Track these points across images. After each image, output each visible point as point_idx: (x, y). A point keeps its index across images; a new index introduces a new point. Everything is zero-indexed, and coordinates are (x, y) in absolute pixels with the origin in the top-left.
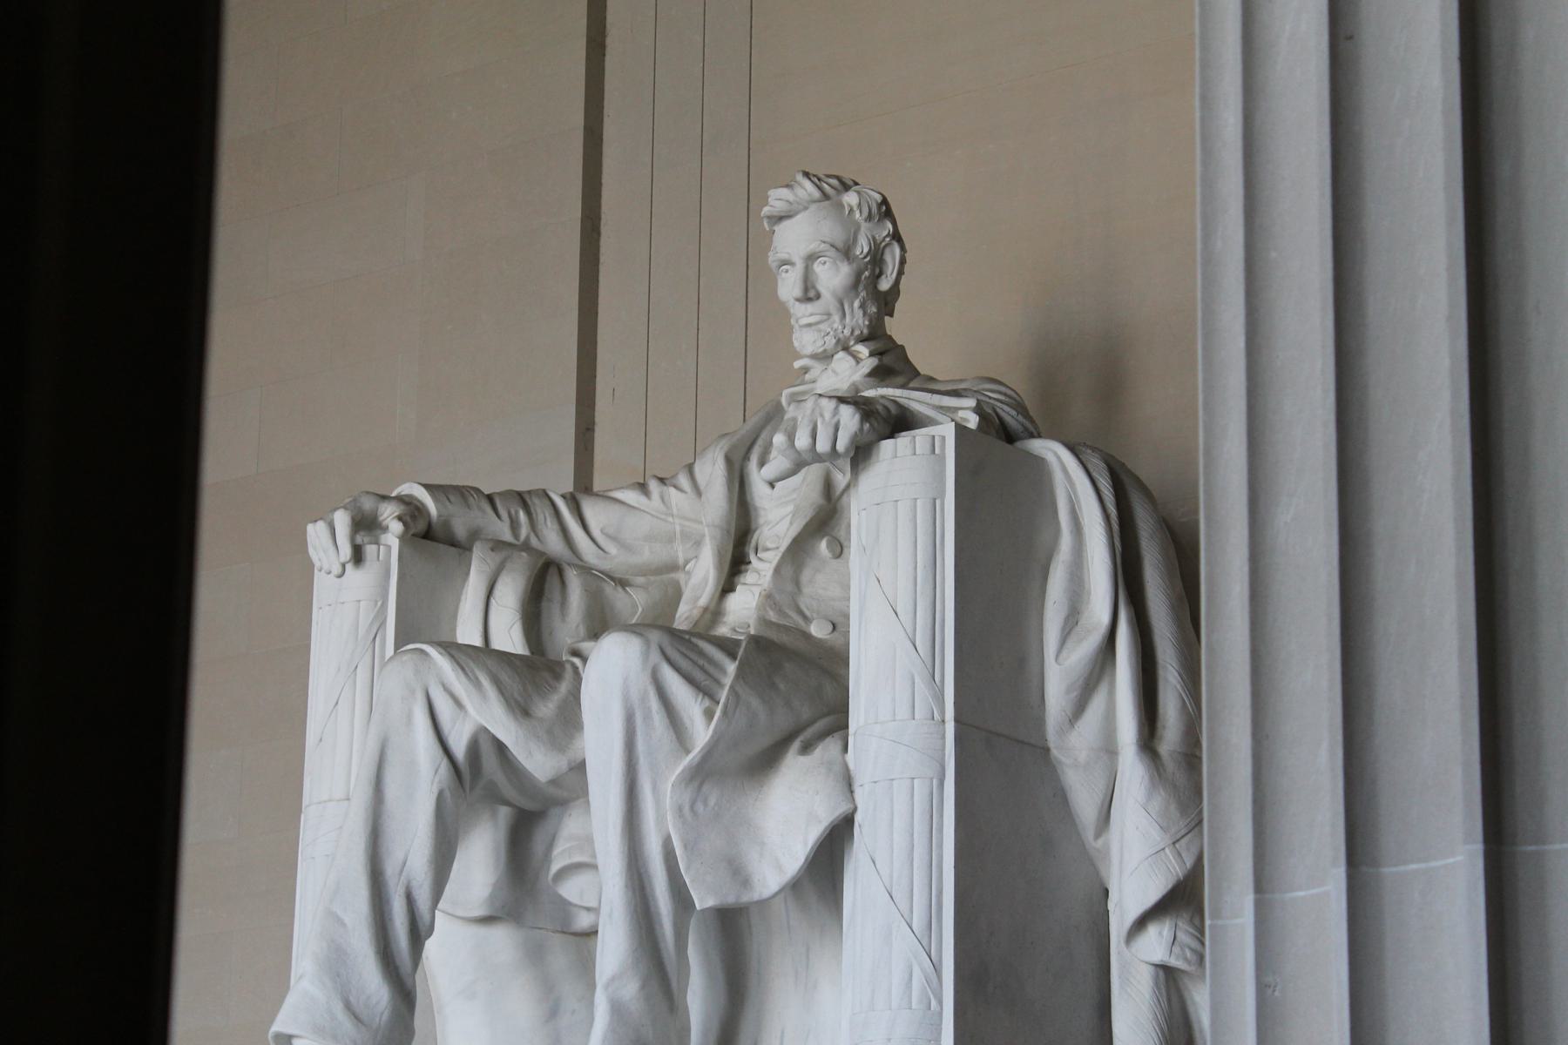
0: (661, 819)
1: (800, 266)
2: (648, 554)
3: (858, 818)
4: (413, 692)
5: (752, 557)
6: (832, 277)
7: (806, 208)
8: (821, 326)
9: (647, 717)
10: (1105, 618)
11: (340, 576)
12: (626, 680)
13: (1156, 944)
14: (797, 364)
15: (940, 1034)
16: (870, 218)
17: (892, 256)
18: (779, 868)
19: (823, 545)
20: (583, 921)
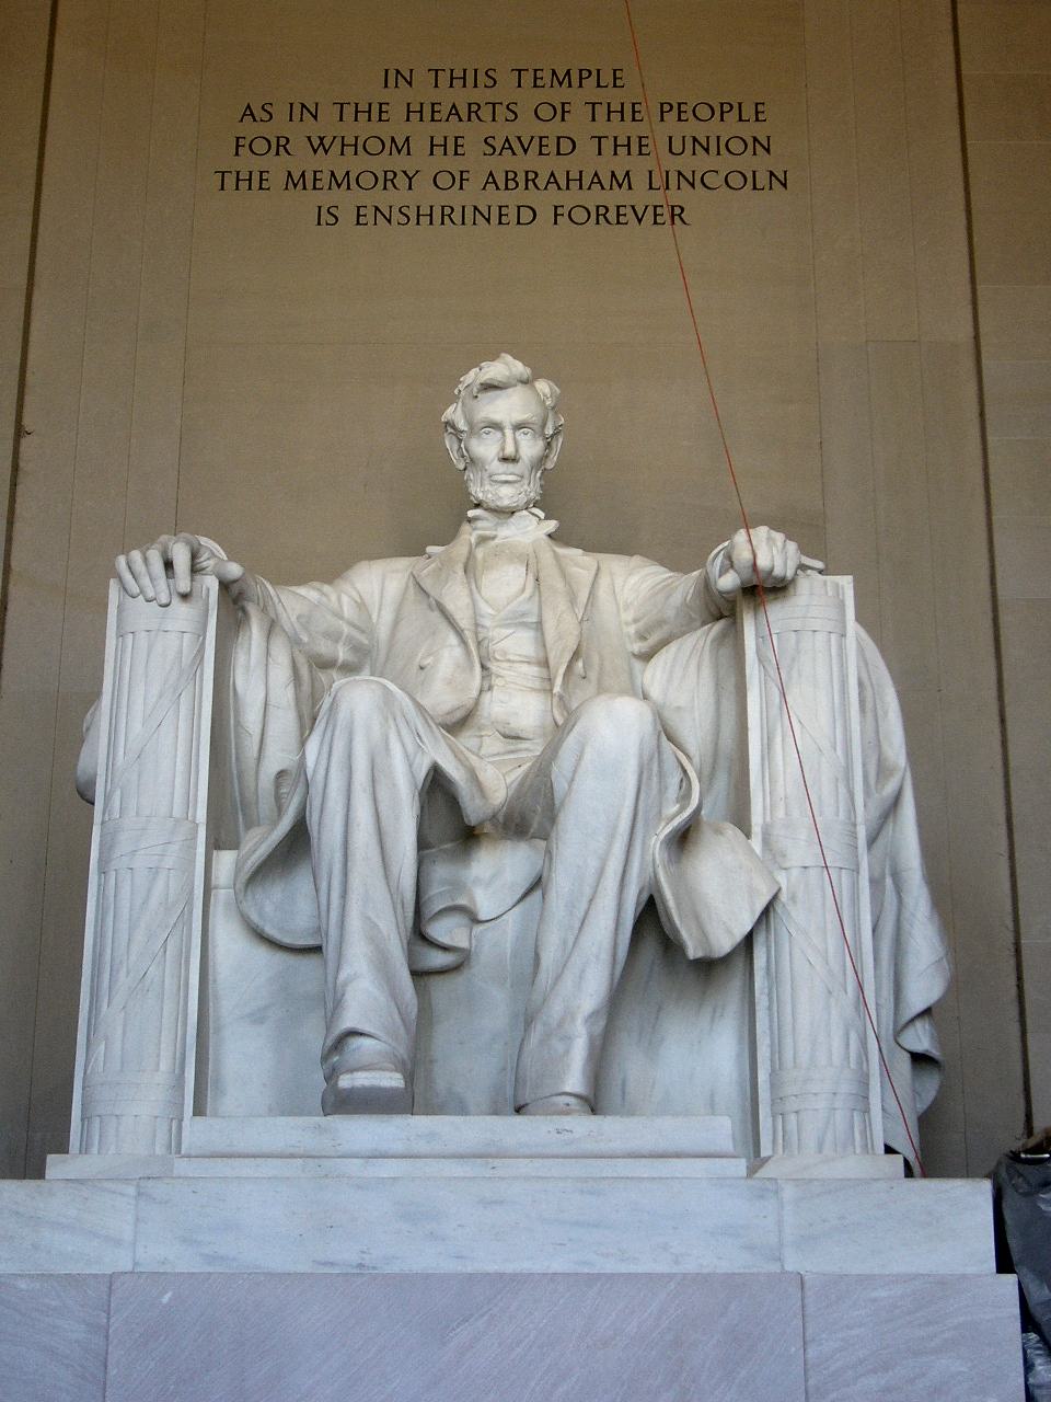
0: (642, 869)
1: (508, 432)
2: (324, 648)
3: (784, 897)
4: (386, 720)
5: (489, 665)
6: (530, 448)
7: (516, 386)
8: (516, 485)
9: (649, 779)
10: (903, 765)
11: (167, 605)
12: (642, 740)
13: (921, 1039)
14: (471, 513)
15: (868, 1089)
16: (553, 408)
17: (559, 442)
18: (729, 931)
19: (580, 664)
20: (438, 959)
